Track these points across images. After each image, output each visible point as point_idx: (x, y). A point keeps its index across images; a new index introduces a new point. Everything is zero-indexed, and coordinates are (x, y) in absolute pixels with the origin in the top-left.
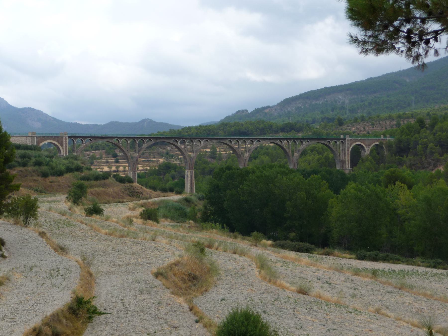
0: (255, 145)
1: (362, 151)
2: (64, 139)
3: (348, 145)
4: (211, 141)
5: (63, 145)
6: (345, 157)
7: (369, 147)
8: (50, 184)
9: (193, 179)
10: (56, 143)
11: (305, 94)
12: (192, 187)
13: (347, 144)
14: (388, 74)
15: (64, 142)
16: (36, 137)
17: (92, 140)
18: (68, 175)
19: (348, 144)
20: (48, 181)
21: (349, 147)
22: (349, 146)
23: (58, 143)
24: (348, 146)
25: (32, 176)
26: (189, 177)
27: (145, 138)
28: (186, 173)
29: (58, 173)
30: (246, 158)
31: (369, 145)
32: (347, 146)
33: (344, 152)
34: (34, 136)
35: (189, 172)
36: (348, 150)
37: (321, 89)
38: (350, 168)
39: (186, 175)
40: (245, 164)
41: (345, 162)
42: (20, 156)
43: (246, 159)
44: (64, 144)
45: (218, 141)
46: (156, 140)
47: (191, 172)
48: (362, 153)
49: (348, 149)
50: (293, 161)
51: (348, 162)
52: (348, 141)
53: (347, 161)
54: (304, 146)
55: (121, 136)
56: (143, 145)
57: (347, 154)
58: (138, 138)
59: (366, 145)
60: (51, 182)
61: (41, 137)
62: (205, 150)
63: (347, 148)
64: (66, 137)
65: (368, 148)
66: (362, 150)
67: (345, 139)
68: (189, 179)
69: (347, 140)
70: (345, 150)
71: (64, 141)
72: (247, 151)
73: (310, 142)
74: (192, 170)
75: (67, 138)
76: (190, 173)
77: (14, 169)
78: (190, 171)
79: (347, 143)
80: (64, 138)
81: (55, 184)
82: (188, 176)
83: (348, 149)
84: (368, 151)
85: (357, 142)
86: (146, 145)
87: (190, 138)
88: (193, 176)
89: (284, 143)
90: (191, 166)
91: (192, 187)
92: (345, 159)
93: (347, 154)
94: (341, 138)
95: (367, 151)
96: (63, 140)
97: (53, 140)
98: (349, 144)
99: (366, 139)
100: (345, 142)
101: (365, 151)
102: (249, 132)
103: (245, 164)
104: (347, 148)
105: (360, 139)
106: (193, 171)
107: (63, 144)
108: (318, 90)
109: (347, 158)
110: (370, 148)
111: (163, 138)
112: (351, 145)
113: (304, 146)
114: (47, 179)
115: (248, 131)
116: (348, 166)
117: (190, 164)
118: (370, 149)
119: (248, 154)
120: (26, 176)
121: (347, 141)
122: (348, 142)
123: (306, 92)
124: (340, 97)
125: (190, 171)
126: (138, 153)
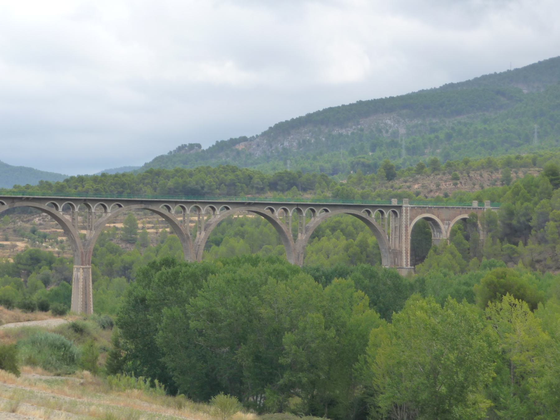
0: (219, 216)
1: (434, 231)
3: (406, 219)
4: (127, 207)
7: (449, 224)
11: (318, 113)
13: (404, 217)
19: (407, 216)
21: (408, 223)
22: (408, 220)
24: (406, 221)
26: (81, 280)
28: (75, 273)
30: (199, 243)
33: (398, 233)
35: (81, 270)
40: (197, 254)
41: (401, 252)
43: (199, 245)
45: (143, 206)
47: (85, 270)
50: (295, 249)
52: (406, 210)
59: (443, 220)
63: (404, 226)
65: (447, 226)
66: (433, 229)
67: (401, 207)
69: (404, 209)
72: (203, 228)
74: (88, 266)
76: (84, 271)
78: (83, 269)
79: (404, 214)
84: (446, 232)
85: (424, 213)
88: (89, 278)
89: (278, 214)
90: (84, 259)
94: (393, 204)
95: (444, 232)
98: (409, 217)
99: (443, 208)
100: (401, 213)
101: (440, 232)
102: (205, 190)
103: (197, 254)
104: (404, 226)
105: (431, 208)
106: (89, 268)
108: (343, 106)
110: (451, 225)
111: (28, 199)
112: (411, 220)
113: (317, 219)
115: (203, 188)
116: (407, 262)
118: (450, 229)
121: (404, 211)
122: (406, 213)
123: (319, 111)
124: (389, 122)
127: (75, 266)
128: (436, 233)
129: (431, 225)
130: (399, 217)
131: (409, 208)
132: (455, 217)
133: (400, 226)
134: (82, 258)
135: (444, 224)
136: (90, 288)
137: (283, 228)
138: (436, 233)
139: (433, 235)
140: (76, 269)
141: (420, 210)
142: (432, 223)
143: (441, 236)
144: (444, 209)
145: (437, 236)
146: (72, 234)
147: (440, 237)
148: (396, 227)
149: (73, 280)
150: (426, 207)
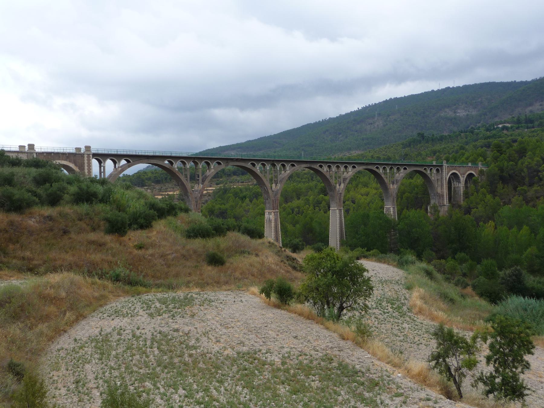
0: (351, 173)
2: (86, 159)
3: (446, 174)
4: (299, 166)
5: (84, 169)
6: (441, 189)
7: (464, 177)
8: (140, 252)
9: (278, 225)
10: (72, 165)
12: (277, 237)
13: (444, 173)
14: (261, 139)
15: (86, 165)
16: (36, 153)
17: (131, 161)
18: (160, 225)
19: (446, 172)
20: (131, 244)
23: (76, 165)
24: (446, 175)
25: (81, 231)
26: (273, 221)
27: (211, 159)
28: (266, 216)
29: (142, 221)
30: (341, 192)
31: (464, 174)
32: (444, 174)
33: (440, 183)
34: (32, 151)
35: (273, 214)
36: (446, 181)
37: (216, 148)
38: (448, 205)
39: (266, 219)
40: (340, 200)
41: (443, 196)
42: (34, 178)
44: (86, 168)
45: (308, 165)
46: (227, 162)
47: (276, 213)
48: (454, 185)
49: (446, 179)
50: (392, 195)
51: (446, 196)
52: (445, 168)
53: (445, 195)
54: (401, 175)
55: (178, 155)
56: (208, 171)
57: (445, 186)
58: (201, 159)
59: (461, 174)
60: (140, 247)
61: (45, 154)
62: (166, 193)
63: (444, 178)
64: (89, 155)
67: (442, 166)
68: (273, 224)
69: (444, 167)
70: (441, 180)
71: (86, 162)
72: (342, 181)
73: (408, 169)
74: (277, 210)
75: (91, 156)
77: (30, 213)
78: (274, 212)
79: (444, 170)
80: (86, 156)
81: (150, 251)
82: (270, 221)
83: (446, 179)
85: (453, 170)
86: (213, 170)
87: (273, 161)
90: (275, 205)
91: (277, 237)
92: (443, 192)
93: (445, 186)
94: (433, 164)
96: (84, 160)
97: (66, 160)
98: (447, 173)
100: (442, 170)
101: (459, 182)
103: (340, 200)
104: (444, 178)
107: (84, 167)
109: (445, 191)
110: (465, 178)
111: (237, 160)
112: (448, 174)
113: (401, 175)
114: (126, 238)
116: (447, 201)
117: (273, 201)
119: (342, 185)
120: (65, 232)
122: (446, 170)
125: (274, 212)
126: (203, 184)
127: (266, 211)
128: (455, 183)
129: (452, 178)
130: (440, 173)
131: (446, 167)
132: (466, 173)
133: (441, 178)
134: (273, 205)
135: (461, 176)
136: (279, 227)
137: (386, 181)
138: (455, 183)
139: (452, 184)
140: (267, 213)
141: (451, 168)
142: (454, 176)
143: (460, 185)
144: (462, 167)
145: (456, 185)
146: (266, 186)
147: (459, 185)
148: (437, 179)
149: (265, 221)
150: (454, 166)
